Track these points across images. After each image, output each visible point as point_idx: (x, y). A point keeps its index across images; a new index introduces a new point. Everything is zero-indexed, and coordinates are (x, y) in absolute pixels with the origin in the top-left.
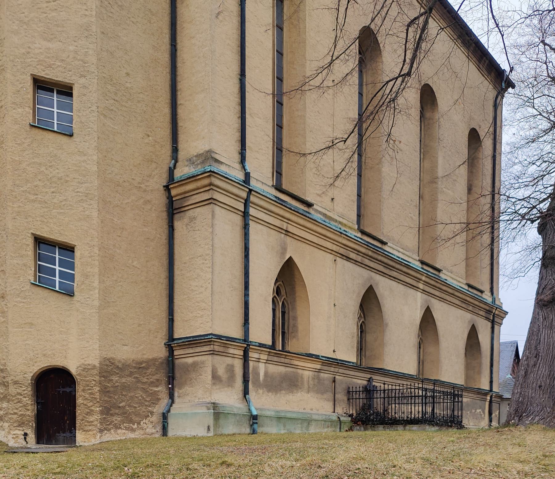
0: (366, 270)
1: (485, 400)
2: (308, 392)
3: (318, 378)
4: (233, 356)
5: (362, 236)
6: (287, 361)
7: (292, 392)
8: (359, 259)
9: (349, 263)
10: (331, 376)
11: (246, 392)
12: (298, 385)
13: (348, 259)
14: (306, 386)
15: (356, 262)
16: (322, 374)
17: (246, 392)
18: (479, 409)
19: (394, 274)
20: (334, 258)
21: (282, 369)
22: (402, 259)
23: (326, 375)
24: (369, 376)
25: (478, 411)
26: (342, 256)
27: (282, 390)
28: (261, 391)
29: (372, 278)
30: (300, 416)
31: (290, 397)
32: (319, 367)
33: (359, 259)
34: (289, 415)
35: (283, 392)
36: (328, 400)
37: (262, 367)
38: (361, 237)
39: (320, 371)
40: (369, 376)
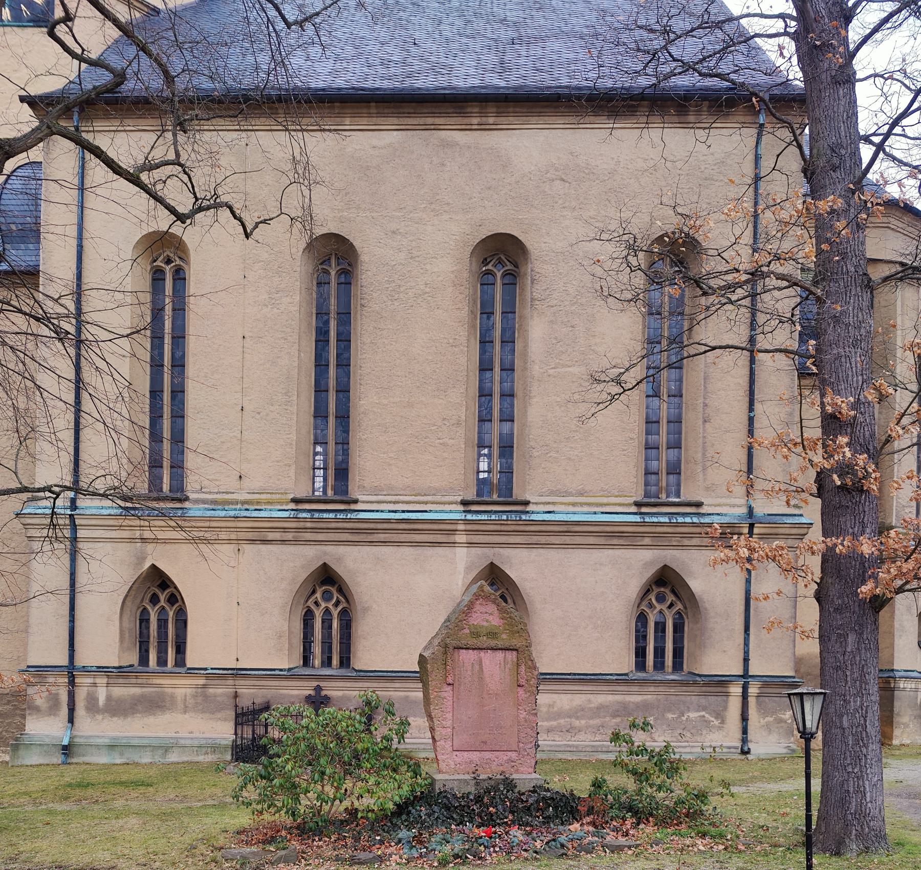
0: (312, 546)
1: (727, 695)
2: (185, 712)
3: (206, 697)
4: (55, 684)
5: (296, 505)
6: (144, 681)
7: (154, 714)
8: (290, 536)
9: (269, 546)
10: (231, 690)
11: (71, 720)
12: (165, 706)
13: (265, 542)
14: (180, 705)
15: (283, 542)
16: (211, 690)
17: (71, 720)
18: (698, 711)
19: (382, 537)
20: (236, 547)
21: (137, 691)
22: (403, 511)
23: (220, 691)
24: (315, 684)
25: (693, 715)
26: (252, 541)
27: (136, 713)
28: (100, 717)
29: (325, 553)
30: (155, 743)
31: (151, 720)
32: (202, 682)
33: (290, 536)
34: (135, 742)
35: (138, 715)
36: (225, 720)
37: (102, 694)
38: (294, 508)
39: (204, 686)
40: (315, 684)
